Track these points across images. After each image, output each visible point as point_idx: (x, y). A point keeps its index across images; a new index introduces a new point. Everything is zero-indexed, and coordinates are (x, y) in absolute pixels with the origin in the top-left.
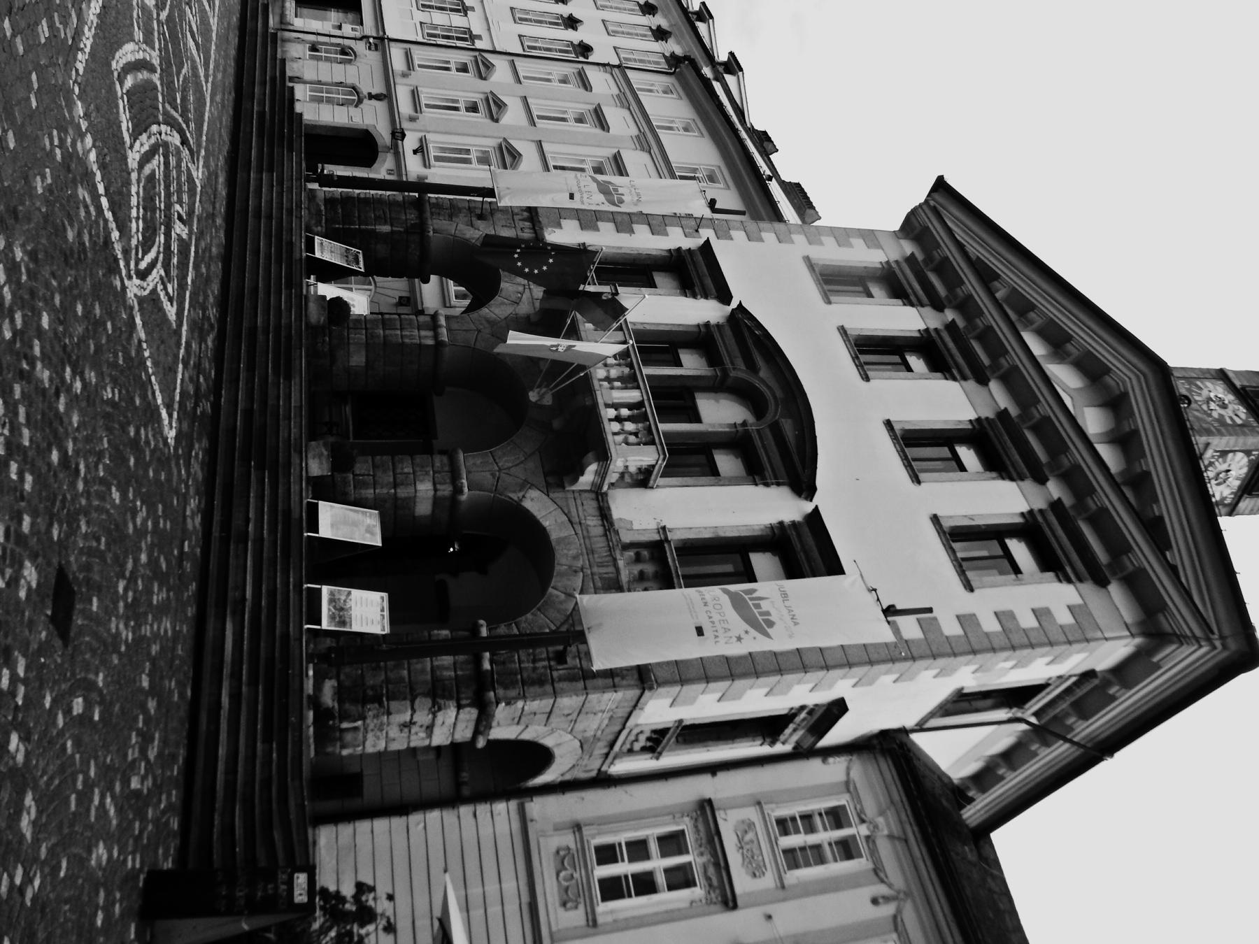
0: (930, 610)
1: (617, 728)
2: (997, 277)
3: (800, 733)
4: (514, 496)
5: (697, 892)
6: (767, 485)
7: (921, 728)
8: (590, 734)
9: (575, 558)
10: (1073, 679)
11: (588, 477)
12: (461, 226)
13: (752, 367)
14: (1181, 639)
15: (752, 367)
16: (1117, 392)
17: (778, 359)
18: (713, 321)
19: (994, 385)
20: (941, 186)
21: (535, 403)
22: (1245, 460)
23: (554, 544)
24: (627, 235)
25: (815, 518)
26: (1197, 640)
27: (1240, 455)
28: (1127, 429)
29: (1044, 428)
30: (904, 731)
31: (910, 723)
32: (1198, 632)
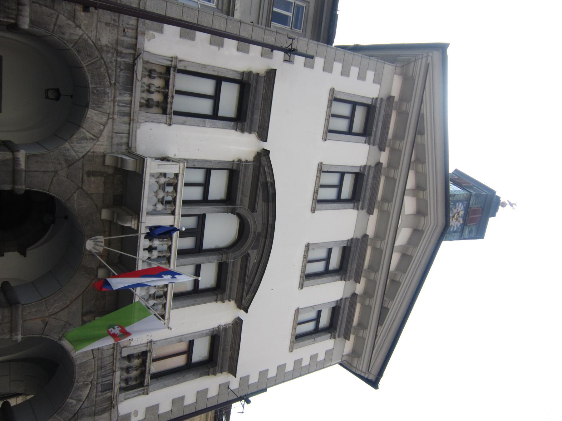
4: (55, 337)
9: (89, 375)
12: (63, 19)
13: (252, 208)
15: (252, 208)
16: (420, 229)
17: (271, 204)
18: (243, 159)
19: (373, 219)
21: (90, 252)
23: (77, 368)
24: (217, 48)
25: (238, 323)
28: (409, 254)
29: (378, 253)
32: (364, 370)
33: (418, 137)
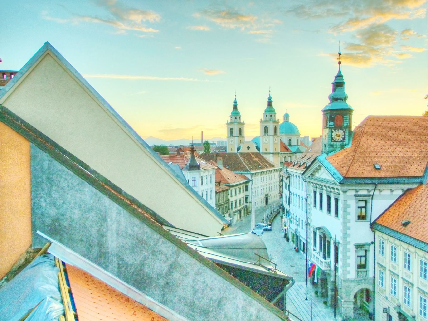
27: (333, 134)
31: (369, 223)
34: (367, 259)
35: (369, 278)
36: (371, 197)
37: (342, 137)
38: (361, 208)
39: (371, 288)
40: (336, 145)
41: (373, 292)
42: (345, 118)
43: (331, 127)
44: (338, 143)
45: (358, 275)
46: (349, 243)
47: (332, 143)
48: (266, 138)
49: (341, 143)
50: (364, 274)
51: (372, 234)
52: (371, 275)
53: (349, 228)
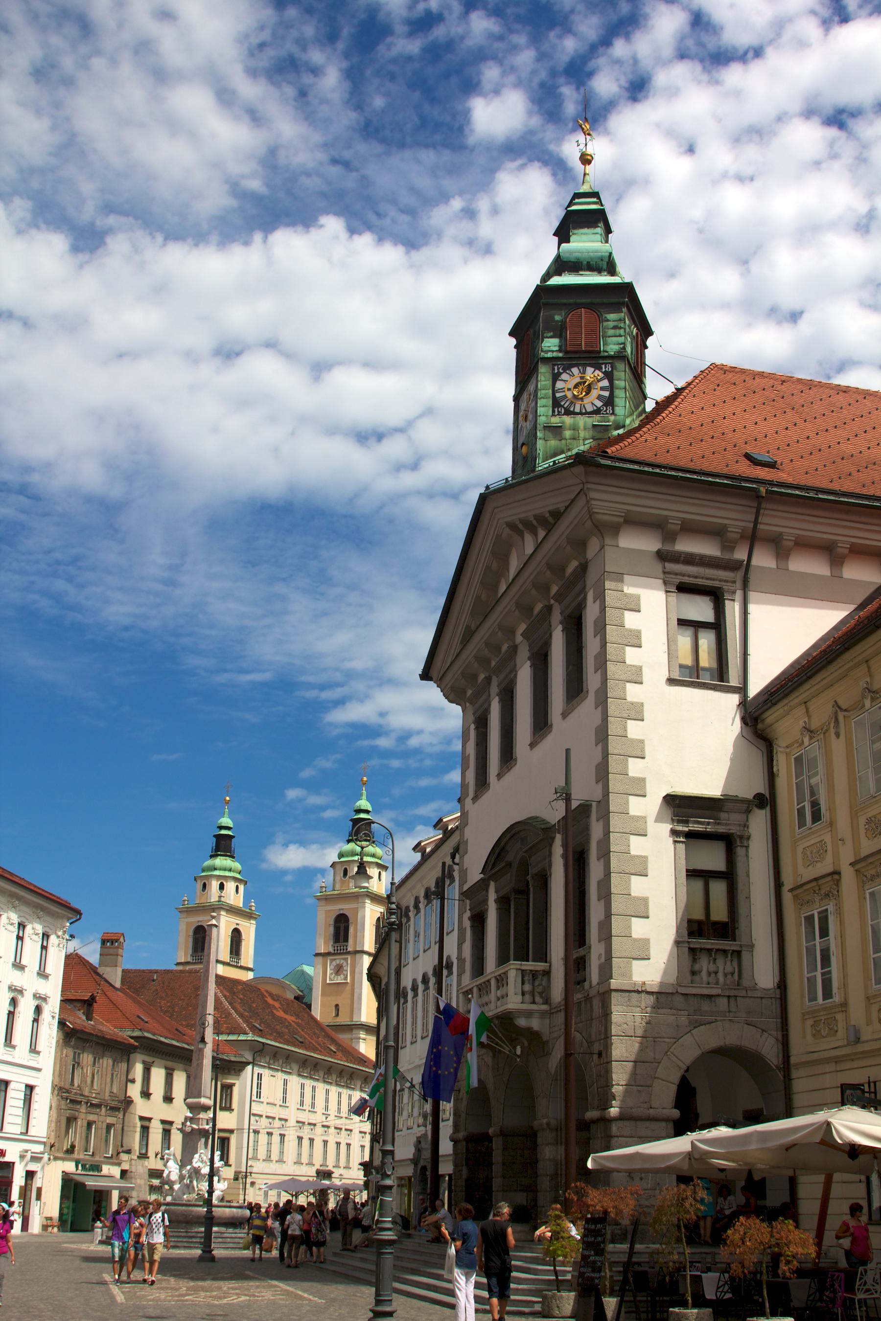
0: (568, 751)
1: (679, 999)
2: (468, 628)
3: (723, 815)
5: (831, 908)
6: (550, 865)
7: (742, 690)
8: (683, 1019)
10: (670, 566)
11: (535, 1024)
14: (591, 515)
20: (426, 675)
22: (564, 376)
26: (588, 502)
27: (559, 385)
30: (744, 704)
31: (735, 698)
33: (473, 627)
34: (741, 886)
35: (755, 988)
36: (740, 574)
37: (599, 397)
38: (696, 626)
39: (769, 1050)
40: (574, 428)
41: (780, 1075)
42: (611, 324)
43: (549, 355)
44: (582, 421)
45: (693, 973)
46: (639, 788)
47: (556, 420)
48: (339, 960)
49: (596, 420)
50: (723, 965)
51: (757, 757)
52: (763, 973)
53: (637, 713)
